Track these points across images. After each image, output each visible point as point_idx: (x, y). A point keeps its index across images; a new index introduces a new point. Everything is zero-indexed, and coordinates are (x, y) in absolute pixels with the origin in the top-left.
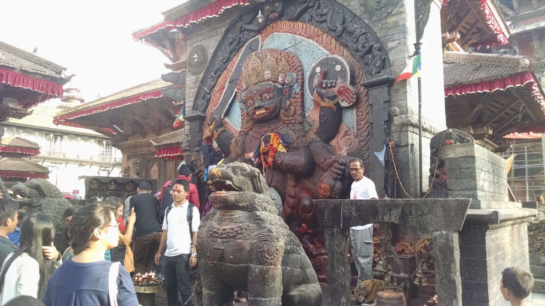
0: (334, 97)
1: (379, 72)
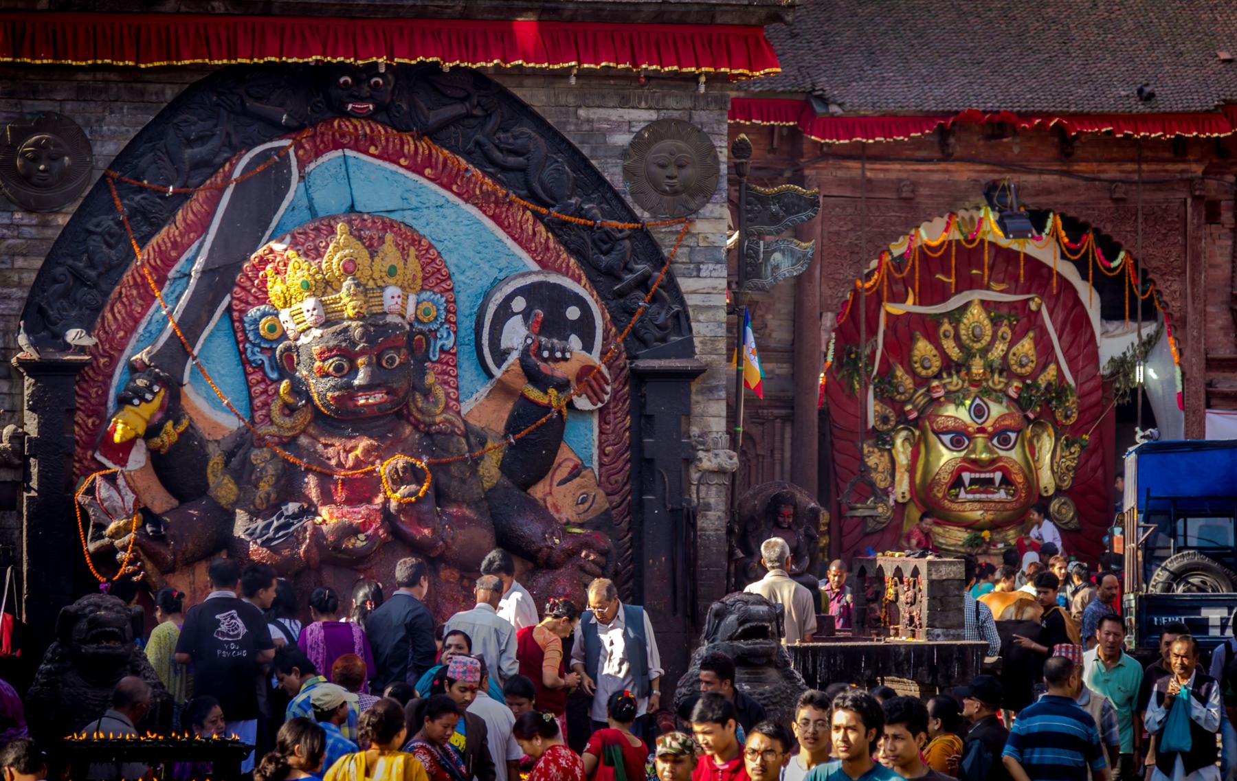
0: (563, 386)
1: (664, 340)
